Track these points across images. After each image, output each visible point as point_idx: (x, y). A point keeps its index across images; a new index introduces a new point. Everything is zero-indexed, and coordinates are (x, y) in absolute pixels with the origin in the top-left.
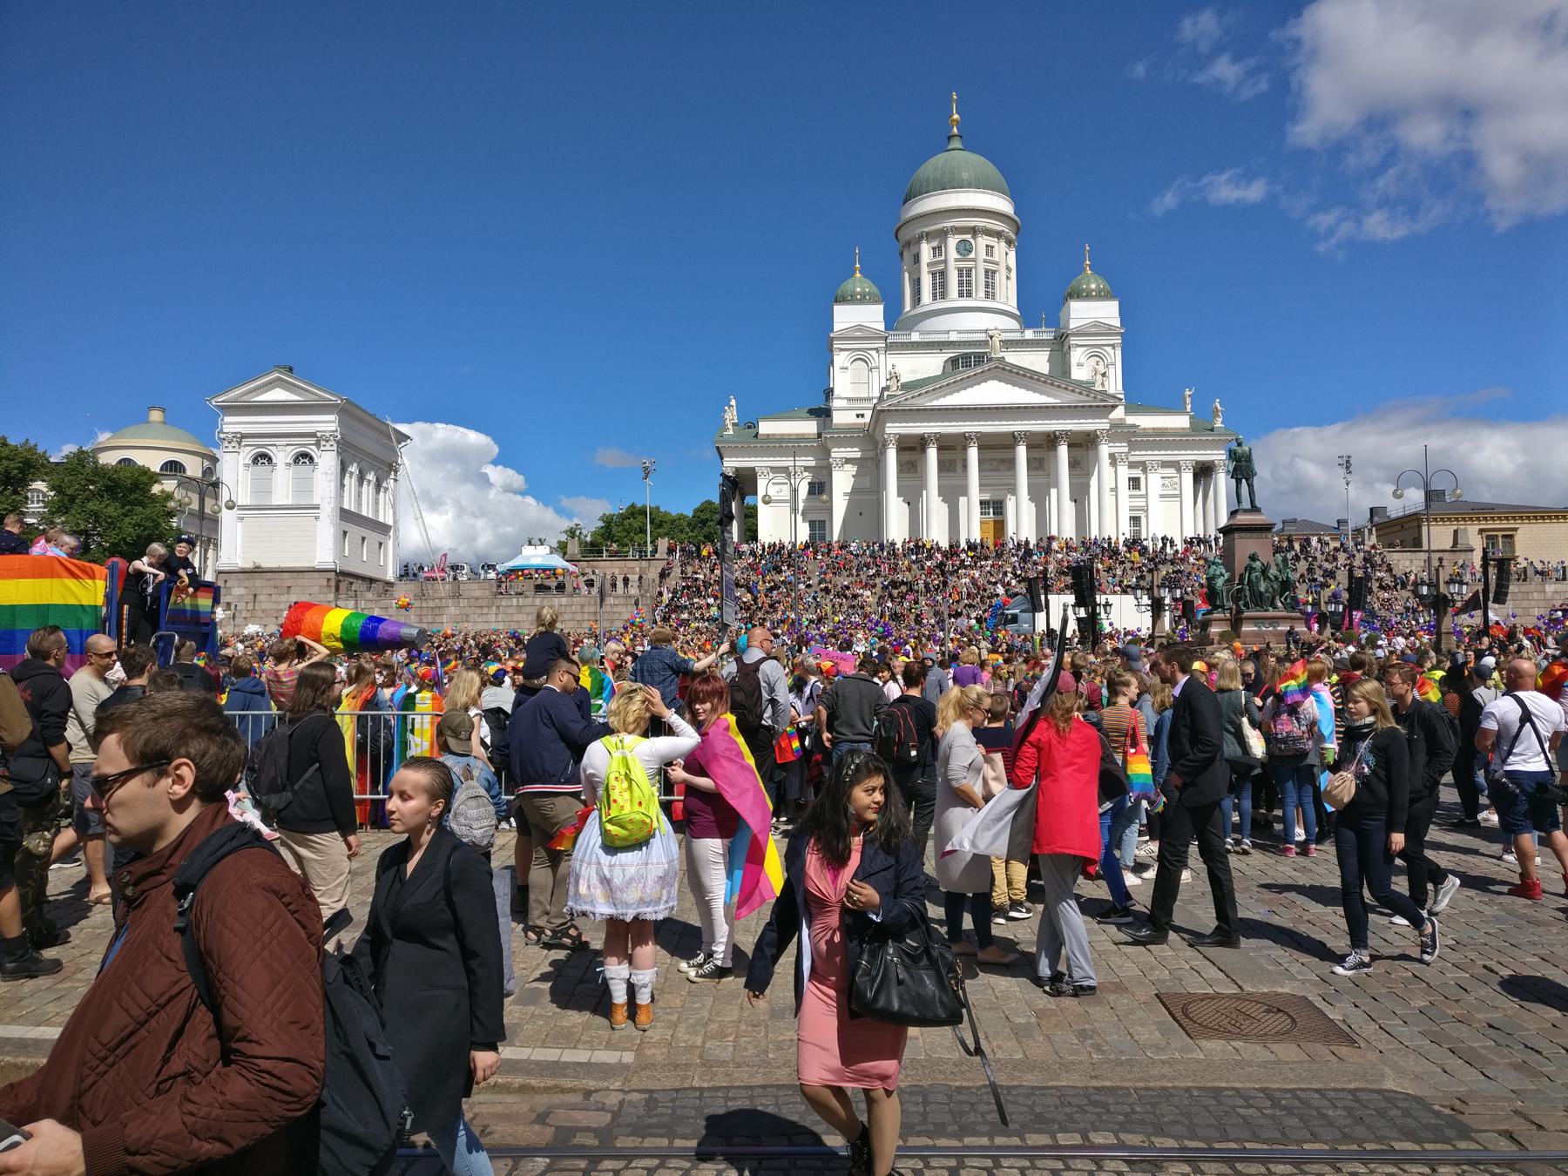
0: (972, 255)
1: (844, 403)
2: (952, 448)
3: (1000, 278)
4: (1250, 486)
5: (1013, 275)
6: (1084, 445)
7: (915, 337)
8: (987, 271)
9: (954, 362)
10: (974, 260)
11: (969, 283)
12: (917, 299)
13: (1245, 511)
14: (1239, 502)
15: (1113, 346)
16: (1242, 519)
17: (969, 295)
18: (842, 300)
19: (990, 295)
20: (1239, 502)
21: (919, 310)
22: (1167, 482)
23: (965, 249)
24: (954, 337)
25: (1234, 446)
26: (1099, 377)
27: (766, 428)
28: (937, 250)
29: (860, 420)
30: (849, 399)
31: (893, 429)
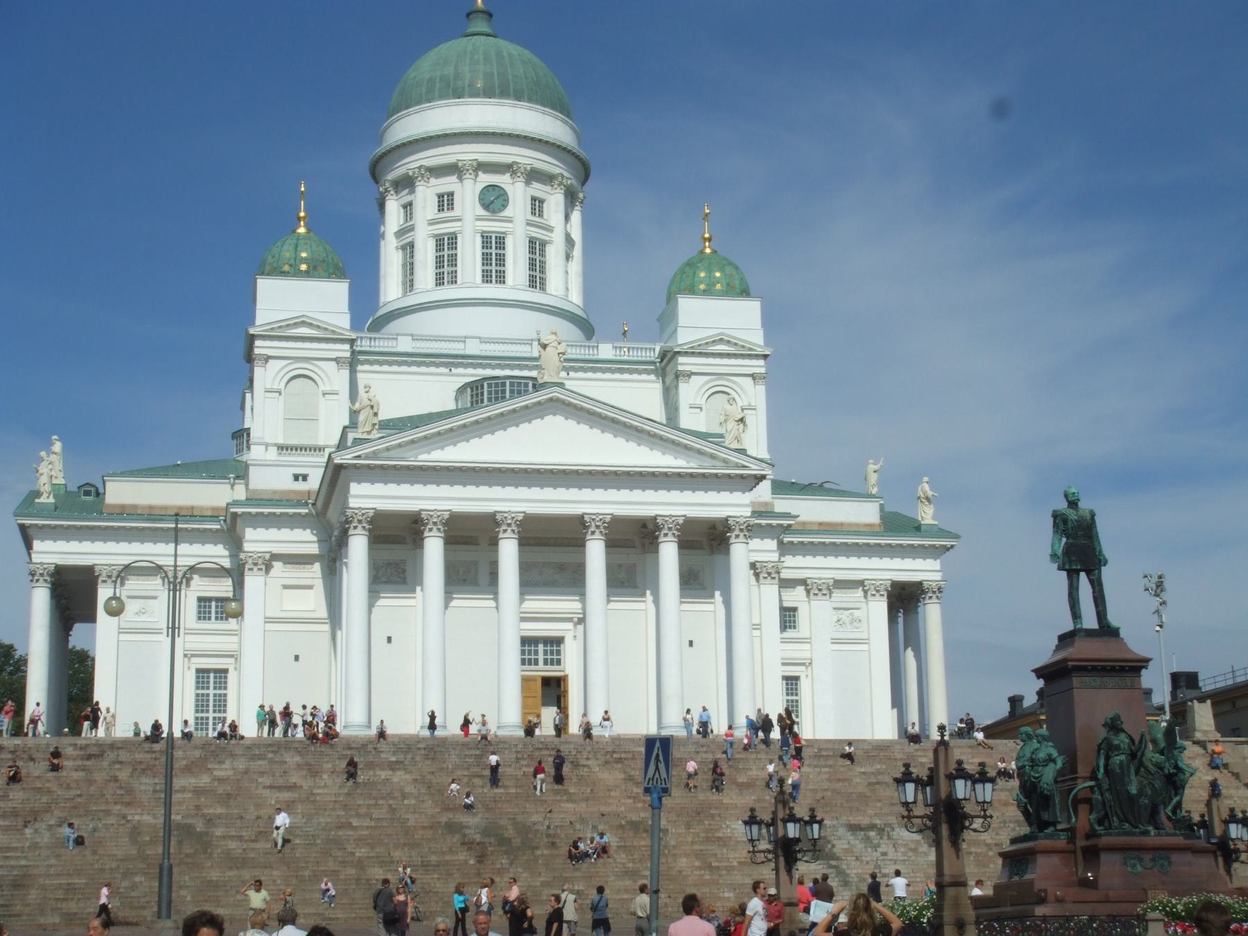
0: (507, 212)
1: (272, 454)
2: (471, 540)
3: (554, 255)
4: (1097, 586)
5: (577, 252)
6: (707, 543)
7: (404, 345)
8: (532, 242)
9: (475, 392)
10: (509, 220)
11: (501, 260)
12: (409, 283)
13: (1090, 633)
14: (1076, 615)
15: (753, 376)
16: (1083, 650)
17: (501, 278)
18: (277, 272)
19: (537, 280)
20: (1076, 615)
21: (412, 300)
22: (844, 615)
23: (493, 200)
24: (473, 348)
25: (1062, 505)
26: (731, 425)
27: (119, 492)
28: (446, 201)
29: (301, 486)
30: (281, 448)
31: (366, 497)
